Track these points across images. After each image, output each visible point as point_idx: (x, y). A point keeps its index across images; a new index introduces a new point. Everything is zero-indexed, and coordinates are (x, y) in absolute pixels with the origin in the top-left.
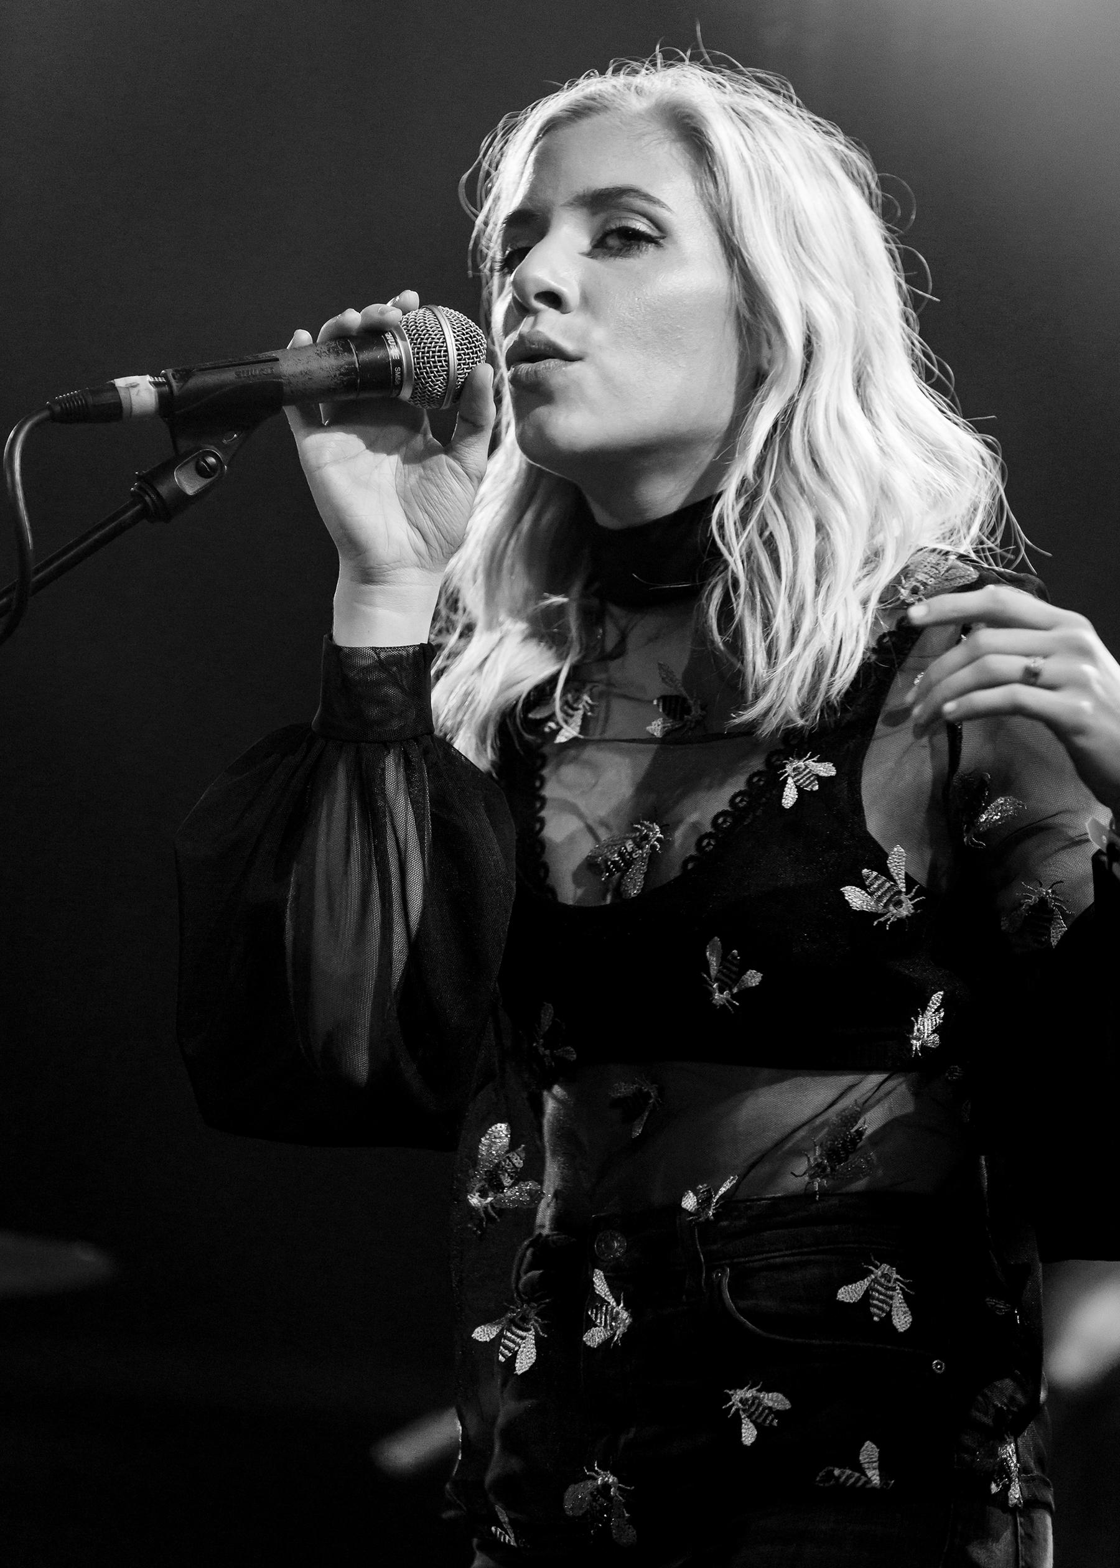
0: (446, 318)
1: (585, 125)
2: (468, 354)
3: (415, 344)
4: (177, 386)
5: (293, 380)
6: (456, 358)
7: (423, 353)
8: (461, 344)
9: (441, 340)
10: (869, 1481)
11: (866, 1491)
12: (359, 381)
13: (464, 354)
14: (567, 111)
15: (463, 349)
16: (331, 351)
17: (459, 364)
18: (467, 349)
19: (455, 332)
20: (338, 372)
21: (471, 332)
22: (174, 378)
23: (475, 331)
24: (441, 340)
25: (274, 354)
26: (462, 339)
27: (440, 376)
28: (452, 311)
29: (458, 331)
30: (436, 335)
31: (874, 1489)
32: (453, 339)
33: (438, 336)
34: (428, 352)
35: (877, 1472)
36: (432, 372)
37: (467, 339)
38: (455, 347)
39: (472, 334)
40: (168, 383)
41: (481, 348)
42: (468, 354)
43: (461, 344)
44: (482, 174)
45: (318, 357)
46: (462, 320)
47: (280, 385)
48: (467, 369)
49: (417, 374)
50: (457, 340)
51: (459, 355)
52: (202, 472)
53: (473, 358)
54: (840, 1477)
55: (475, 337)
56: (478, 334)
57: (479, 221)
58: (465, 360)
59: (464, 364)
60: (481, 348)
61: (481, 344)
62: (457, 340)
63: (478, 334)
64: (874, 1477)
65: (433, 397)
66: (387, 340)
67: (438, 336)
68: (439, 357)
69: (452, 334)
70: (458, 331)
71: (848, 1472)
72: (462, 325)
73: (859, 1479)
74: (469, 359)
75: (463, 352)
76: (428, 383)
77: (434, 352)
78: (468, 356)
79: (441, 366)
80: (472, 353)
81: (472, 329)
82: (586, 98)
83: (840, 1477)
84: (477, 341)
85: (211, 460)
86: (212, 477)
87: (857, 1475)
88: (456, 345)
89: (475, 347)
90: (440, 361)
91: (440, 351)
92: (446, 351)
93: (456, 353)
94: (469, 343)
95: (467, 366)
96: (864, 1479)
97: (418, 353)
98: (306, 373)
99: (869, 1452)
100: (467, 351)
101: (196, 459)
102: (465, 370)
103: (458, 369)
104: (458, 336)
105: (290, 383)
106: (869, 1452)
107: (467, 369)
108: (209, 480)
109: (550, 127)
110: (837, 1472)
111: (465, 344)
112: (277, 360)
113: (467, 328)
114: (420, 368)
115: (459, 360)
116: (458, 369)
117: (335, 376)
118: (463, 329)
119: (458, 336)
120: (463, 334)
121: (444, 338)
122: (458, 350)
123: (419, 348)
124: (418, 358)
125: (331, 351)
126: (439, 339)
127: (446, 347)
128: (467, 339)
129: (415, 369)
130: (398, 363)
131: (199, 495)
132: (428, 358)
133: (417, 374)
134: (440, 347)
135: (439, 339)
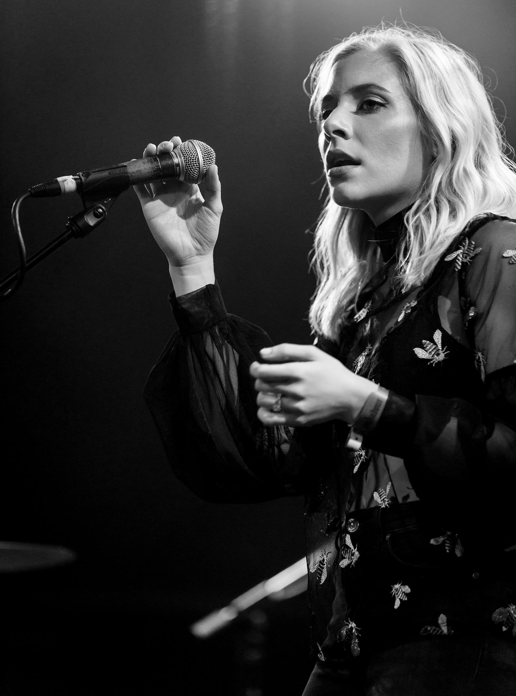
1: (352, 57)
10: (442, 631)
11: (442, 636)
14: (344, 51)
31: (445, 635)
35: (446, 627)
44: (312, 79)
54: (430, 630)
57: (312, 99)
64: (445, 629)
71: (434, 628)
73: (438, 631)
82: (352, 45)
83: (430, 630)
87: (438, 629)
96: (440, 631)
99: (442, 619)
106: (442, 619)
109: (340, 57)
110: (429, 628)
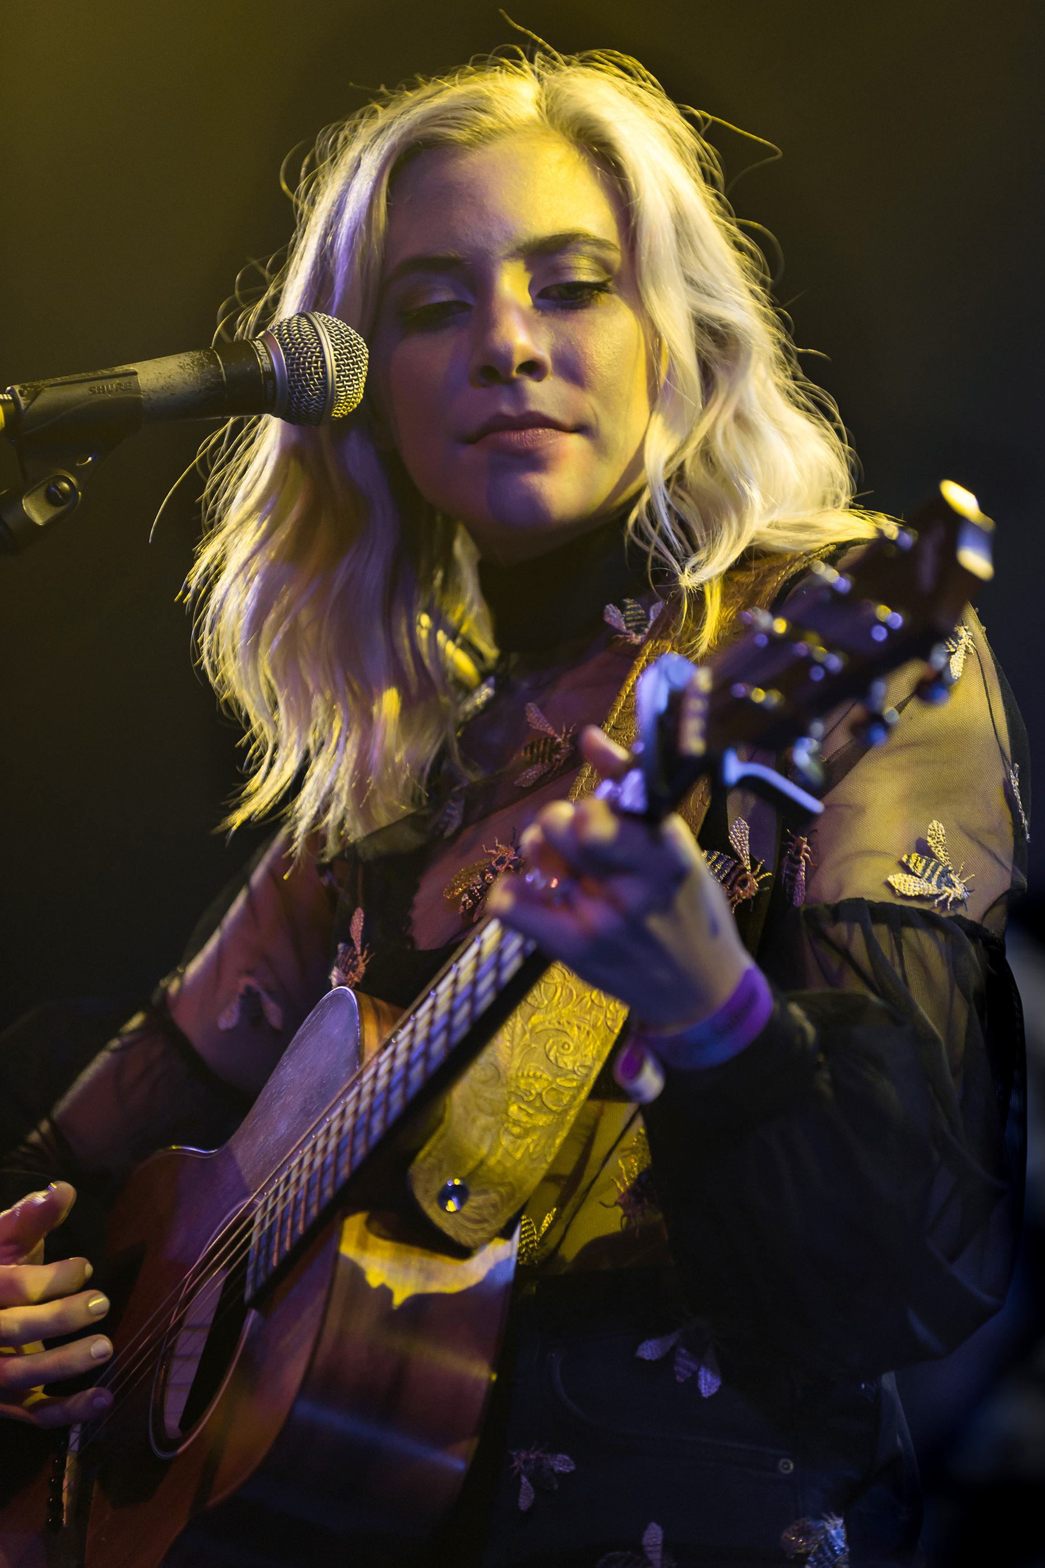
0: (324, 327)
2: (348, 365)
3: (289, 354)
4: (25, 404)
5: (153, 396)
6: (335, 369)
7: (298, 364)
8: (340, 354)
9: (318, 349)
12: (226, 397)
13: (344, 365)
15: (342, 360)
16: (196, 363)
17: (338, 377)
18: (347, 359)
19: (332, 341)
20: (203, 387)
21: (351, 339)
22: (22, 395)
23: (355, 339)
24: (318, 349)
25: (132, 367)
26: (342, 349)
27: (317, 389)
28: (330, 317)
29: (337, 339)
30: (312, 344)
32: (332, 349)
33: (315, 345)
34: (304, 363)
36: (308, 386)
37: (346, 348)
38: (333, 358)
39: (352, 343)
40: (15, 401)
41: (363, 357)
42: (348, 365)
43: (340, 354)
45: (182, 371)
46: (341, 327)
47: (140, 399)
48: (347, 381)
49: (291, 387)
50: (335, 350)
51: (338, 366)
52: (52, 498)
53: (353, 370)
55: (355, 345)
56: (358, 343)
58: (344, 371)
59: (344, 376)
60: (363, 357)
61: (362, 354)
62: (335, 350)
63: (358, 343)
65: (311, 413)
66: (258, 350)
67: (315, 345)
68: (316, 368)
69: (330, 343)
70: (337, 339)
72: (341, 332)
74: (349, 370)
75: (342, 362)
76: (304, 397)
77: (309, 363)
78: (348, 367)
79: (317, 379)
80: (353, 364)
81: (352, 337)
84: (358, 350)
85: (66, 486)
86: (63, 505)
88: (335, 355)
89: (356, 357)
90: (317, 373)
91: (316, 362)
92: (324, 362)
93: (334, 363)
94: (349, 352)
95: (347, 378)
97: (292, 365)
98: (168, 388)
100: (346, 361)
101: (46, 485)
102: (345, 383)
103: (338, 382)
104: (337, 344)
105: (150, 399)
107: (347, 381)
108: (63, 508)
111: (344, 354)
112: (135, 373)
113: (346, 336)
114: (294, 382)
115: (338, 371)
116: (338, 382)
117: (200, 391)
118: (342, 337)
119: (337, 344)
120: (343, 343)
121: (322, 348)
122: (337, 360)
123: (293, 359)
124: (292, 370)
125: (196, 363)
126: (315, 348)
127: (324, 357)
128: (346, 348)
129: (289, 382)
130: (270, 375)
131: (48, 525)
132: (303, 369)
133: (291, 387)
134: (317, 357)
135: (315, 348)
